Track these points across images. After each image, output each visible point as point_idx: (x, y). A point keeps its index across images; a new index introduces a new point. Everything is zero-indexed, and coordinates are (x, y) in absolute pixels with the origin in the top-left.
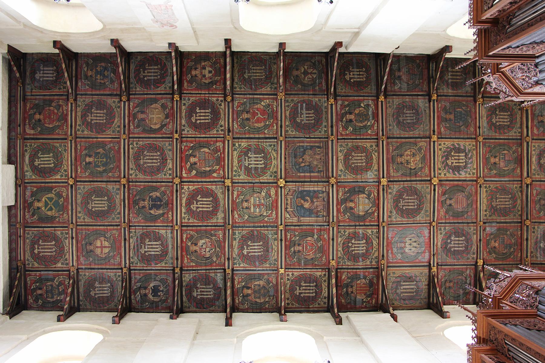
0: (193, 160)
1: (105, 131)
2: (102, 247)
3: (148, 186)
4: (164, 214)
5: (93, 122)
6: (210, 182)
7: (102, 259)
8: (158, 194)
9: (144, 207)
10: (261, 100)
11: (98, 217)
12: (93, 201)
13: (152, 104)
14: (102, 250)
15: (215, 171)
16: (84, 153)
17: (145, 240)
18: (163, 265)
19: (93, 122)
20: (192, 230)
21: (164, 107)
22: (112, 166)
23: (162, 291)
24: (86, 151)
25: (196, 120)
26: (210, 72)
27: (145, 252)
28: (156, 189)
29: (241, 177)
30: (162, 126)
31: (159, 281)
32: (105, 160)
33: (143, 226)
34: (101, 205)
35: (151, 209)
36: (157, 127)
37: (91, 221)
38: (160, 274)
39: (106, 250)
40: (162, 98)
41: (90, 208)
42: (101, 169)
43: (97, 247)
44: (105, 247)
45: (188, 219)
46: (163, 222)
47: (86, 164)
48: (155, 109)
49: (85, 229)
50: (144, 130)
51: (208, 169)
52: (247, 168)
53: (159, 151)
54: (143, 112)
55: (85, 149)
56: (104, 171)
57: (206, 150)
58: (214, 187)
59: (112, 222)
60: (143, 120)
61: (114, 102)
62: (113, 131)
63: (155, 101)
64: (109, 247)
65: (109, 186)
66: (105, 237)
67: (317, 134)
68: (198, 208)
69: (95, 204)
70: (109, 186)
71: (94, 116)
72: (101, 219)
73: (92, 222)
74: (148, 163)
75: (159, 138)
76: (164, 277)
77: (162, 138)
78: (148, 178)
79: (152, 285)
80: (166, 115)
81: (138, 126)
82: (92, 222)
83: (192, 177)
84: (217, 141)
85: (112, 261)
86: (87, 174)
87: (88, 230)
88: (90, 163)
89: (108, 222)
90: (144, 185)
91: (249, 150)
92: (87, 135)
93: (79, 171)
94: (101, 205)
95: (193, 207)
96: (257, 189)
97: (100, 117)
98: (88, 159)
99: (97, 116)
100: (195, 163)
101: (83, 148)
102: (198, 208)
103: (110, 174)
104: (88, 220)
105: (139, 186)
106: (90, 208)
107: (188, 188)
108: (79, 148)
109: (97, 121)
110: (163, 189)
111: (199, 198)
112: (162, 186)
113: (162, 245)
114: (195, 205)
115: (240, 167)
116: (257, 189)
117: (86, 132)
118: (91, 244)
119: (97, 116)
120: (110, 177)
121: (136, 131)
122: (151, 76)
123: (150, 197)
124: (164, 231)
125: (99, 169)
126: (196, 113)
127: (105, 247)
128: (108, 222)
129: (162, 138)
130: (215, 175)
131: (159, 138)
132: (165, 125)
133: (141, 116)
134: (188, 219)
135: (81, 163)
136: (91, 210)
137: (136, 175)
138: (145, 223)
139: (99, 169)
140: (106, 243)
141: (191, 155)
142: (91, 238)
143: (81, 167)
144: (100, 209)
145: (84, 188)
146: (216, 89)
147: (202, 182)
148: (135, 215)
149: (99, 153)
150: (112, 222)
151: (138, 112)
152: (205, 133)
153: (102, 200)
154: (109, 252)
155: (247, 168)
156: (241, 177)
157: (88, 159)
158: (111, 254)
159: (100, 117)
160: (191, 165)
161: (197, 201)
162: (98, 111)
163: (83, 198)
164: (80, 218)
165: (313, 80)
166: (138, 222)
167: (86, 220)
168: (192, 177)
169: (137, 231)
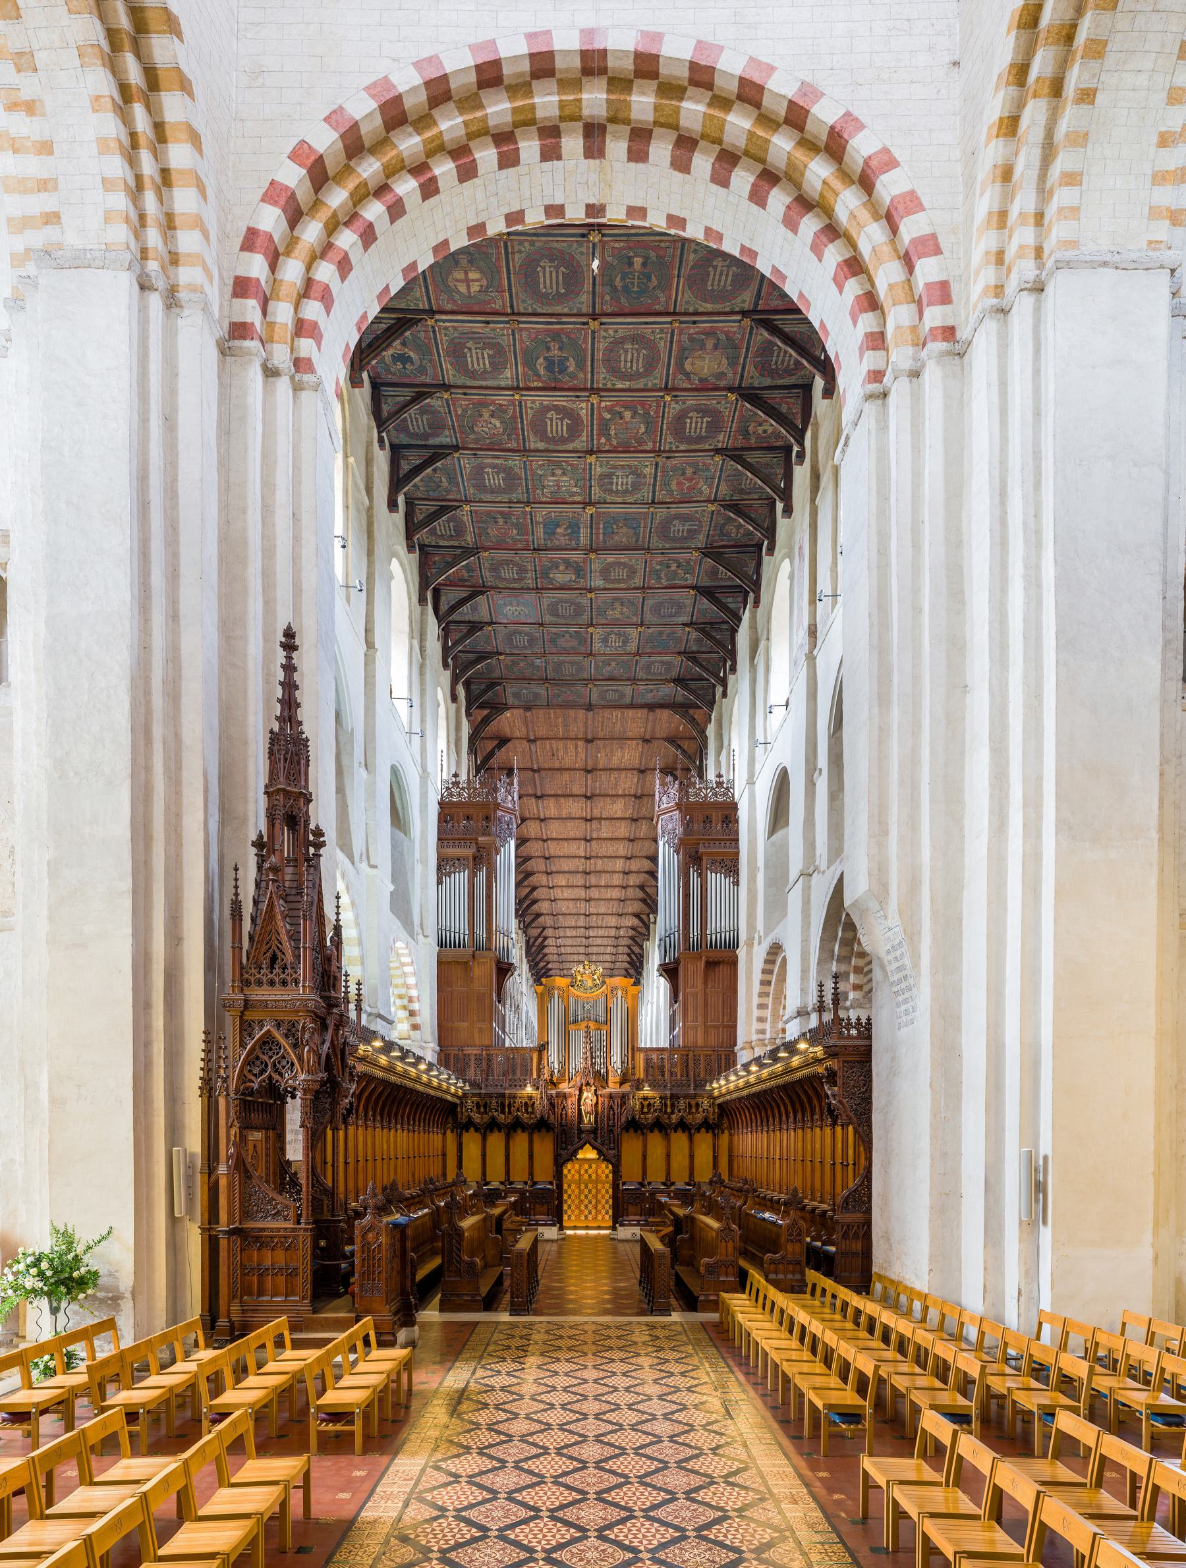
0: (628, 415)
1: (690, 288)
2: (467, 281)
3: (585, 355)
4: (539, 376)
5: (711, 269)
6: (592, 435)
7: (445, 283)
8: (571, 369)
9: (548, 349)
10: (710, 487)
11: (526, 275)
12: (557, 268)
13: (728, 358)
14: (461, 281)
15: (608, 440)
16: (652, 254)
17: (490, 349)
18: (451, 372)
19: (711, 269)
20: (514, 412)
21: (721, 376)
22: (623, 300)
23: (404, 368)
24: (654, 258)
25: (691, 418)
26: (765, 431)
27: (470, 349)
28: (581, 365)
29: (599, 469)
30: (687, 375)
31: (421, 365)
32: (635, 289)
33: (514, 345)
34: (548, 282)
35: (545, 359)
36: (688, 367)
37: (517, 265)
38: (435, 367)
39: (462, 288)
40: (735, 373)
41: (542, 264)
42: (618, 282)
43: (466, 274)
44: (468, 287)
45: (532, 408)
46: (525, 374)
47: (630, 258)
48: (719, 364)
49: (499, 253)
50: (685, 349)
51: (612, 432)
52: (610, 475)
53: (646, 370)
54: (716, 347)
55: (659, 257)
56: (614, 289)
57: (643, 430)
58: (584, 438)
59: (517, 298)
60: (703, 347)
61: (744, 302)
62: (687, 302)
63: (733, 363)
64: (469, 292)
65: (585, 296)
66: (487, 288)
67: (654, 538)
68: (551, 420)
69: (551, 273)
70: (585, 296)
71: (722, 271)
72: (523, 281)
73: (514, 266)
74: (626, 356)
75: (668, 371)
76: (430, 371)
77: (668, 375)
78: (599, 355)
79: (412, 354)
80: (706, 379)
81: (692, 340)
82: (514, 266)
83: (599, 414)
84: (654, 442)
85: (443, 297)
86: (609, 259)
87: (498, 259)
88: (631, 264)
89: (517, 294)
90: (586, 350)
91: (639, 476)
92: (687, 260)
93: (617, 245)
94: (548, 282)
95: (552, 414)
96: (580, 483)
97: (719, 281)
98: (638, 261)
99: (721, 275)
100: (621, 418)
101: (661, 253)
102: (551, 420)
103: (607, 298)
104: (518, 259)
105: (585, 341)
106: (542, 264)
107: (583, 409)
108: (662, 245)
109: (711, 277)
110: (581, 375)
111: (566, 421)
112: (585, 374)
113: (485, 372)
114: (555, 417)
115: (614, 467)
116: (580, 483)
117: (692, 257)
118: (471, 262)
119: (721, 275)
120: (602, 298)
121: (685, 338)
122: (778, 356)
123: (567, 359)
124: (509, 375)
125: (618, 279)
126: (702, 418)
127: (468, 287)
128: (517, 294)
129: (668, 375)
130: (603, 440)
131: (668, 371)
132: (689, 379)
133: (710, 344)
134: (532, 408)
135: (630, 248)
136: (538, 265)
137: (605, 338)
138: (521, 349)
139: (618, 279)
140: (478, 289)
141: (635, 413)
142: (482, 264)
143: (623, 248)
144: (541, 280)
145: (582, 253)
146: (736, 439)
147: (592, 425)
148: (533, 336)
149: (649, 279)
150: (517, 298)
151: (718, 339)
152: (668, 429)
153: (557, 284)
154: (459, 292)
155: (610, 475)
156: (599, 469)
157: (638, 261)
158: (457, 297)
159: (719, 281)
160: (620, 413)
161: (562, 420)
162: (730, 277)
163: (562, 252)
164: (521, 243)
165: (728, 534)
166: (521, 341)
167: (517, 256)
168: (599, 414)
169: (505, 338)
